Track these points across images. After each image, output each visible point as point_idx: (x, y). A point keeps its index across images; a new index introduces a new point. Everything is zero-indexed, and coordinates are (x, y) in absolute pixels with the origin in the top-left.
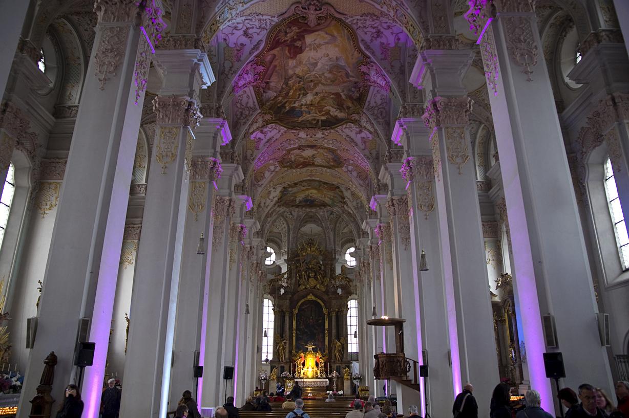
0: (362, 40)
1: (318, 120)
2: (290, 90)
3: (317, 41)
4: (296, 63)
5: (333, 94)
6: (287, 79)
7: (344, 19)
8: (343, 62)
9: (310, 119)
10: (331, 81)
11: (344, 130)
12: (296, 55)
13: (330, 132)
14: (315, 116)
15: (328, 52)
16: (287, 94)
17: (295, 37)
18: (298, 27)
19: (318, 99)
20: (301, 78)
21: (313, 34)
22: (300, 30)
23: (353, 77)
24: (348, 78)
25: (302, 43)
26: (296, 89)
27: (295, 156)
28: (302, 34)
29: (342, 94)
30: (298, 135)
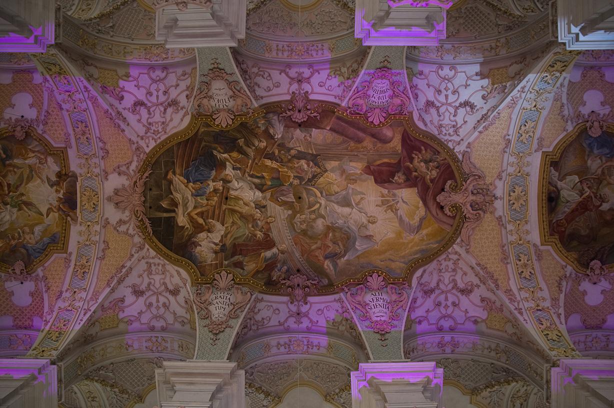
0: (424, 271)
1: (174, 211)
2: (282, 161)
3: (404, 205)
4: (357, 174)
5: (266, 235)
6: (314, 159)
7: (459, 240)
8: (365, 246)
9: (178, 196)
10: (304, 233)
11: (143, 261)
12: (373, 174)
13: (132, 236)
14: (185, 206)
15: (380, 222)
16: (271, 157)
17: (414, 173)
18: (435, 178)
19: (245, 210)
20: (310, 180)
21: (419, 199)
22: (429, 181)
23: (335, 265)
24: (326, 258)
25: (399, 184)
26: (279, 171)
27: (30, 166)
28: (420, 185)
29: (275, 250)
30: (119, 174)
